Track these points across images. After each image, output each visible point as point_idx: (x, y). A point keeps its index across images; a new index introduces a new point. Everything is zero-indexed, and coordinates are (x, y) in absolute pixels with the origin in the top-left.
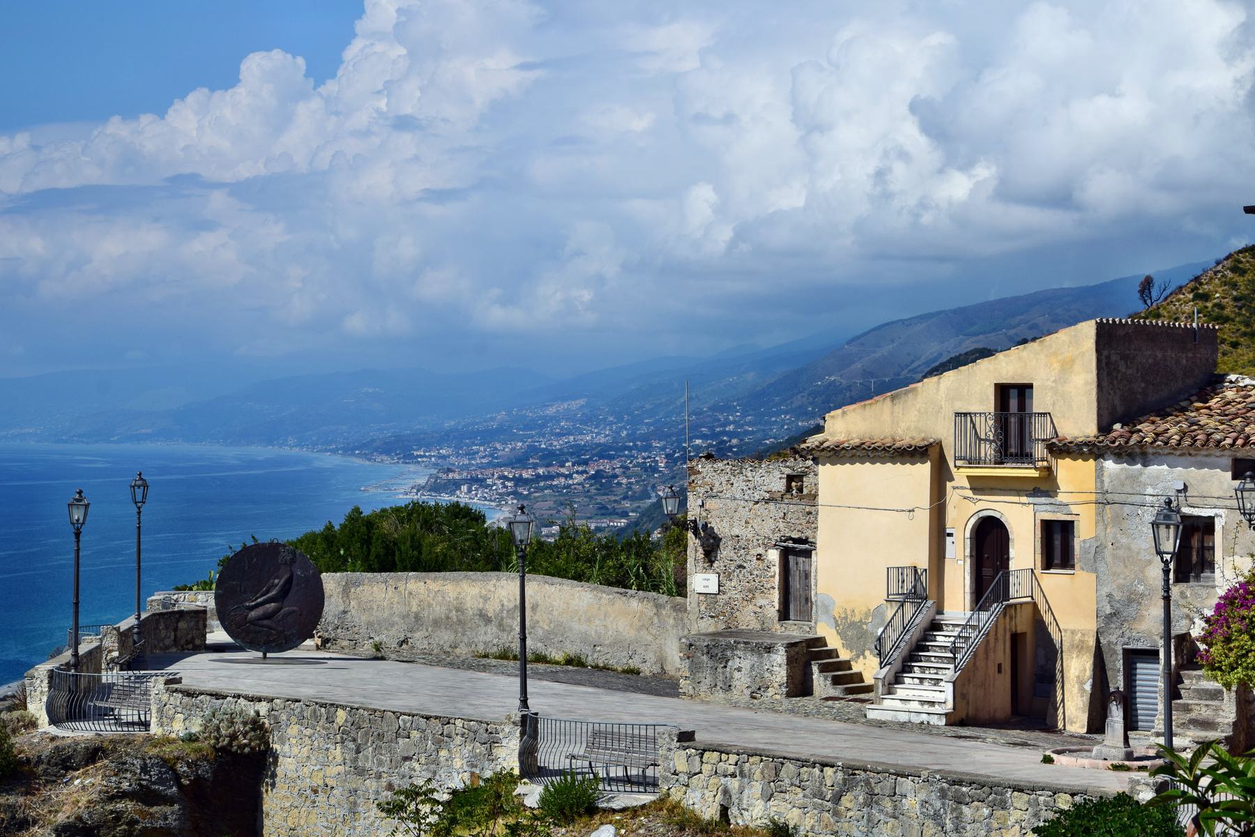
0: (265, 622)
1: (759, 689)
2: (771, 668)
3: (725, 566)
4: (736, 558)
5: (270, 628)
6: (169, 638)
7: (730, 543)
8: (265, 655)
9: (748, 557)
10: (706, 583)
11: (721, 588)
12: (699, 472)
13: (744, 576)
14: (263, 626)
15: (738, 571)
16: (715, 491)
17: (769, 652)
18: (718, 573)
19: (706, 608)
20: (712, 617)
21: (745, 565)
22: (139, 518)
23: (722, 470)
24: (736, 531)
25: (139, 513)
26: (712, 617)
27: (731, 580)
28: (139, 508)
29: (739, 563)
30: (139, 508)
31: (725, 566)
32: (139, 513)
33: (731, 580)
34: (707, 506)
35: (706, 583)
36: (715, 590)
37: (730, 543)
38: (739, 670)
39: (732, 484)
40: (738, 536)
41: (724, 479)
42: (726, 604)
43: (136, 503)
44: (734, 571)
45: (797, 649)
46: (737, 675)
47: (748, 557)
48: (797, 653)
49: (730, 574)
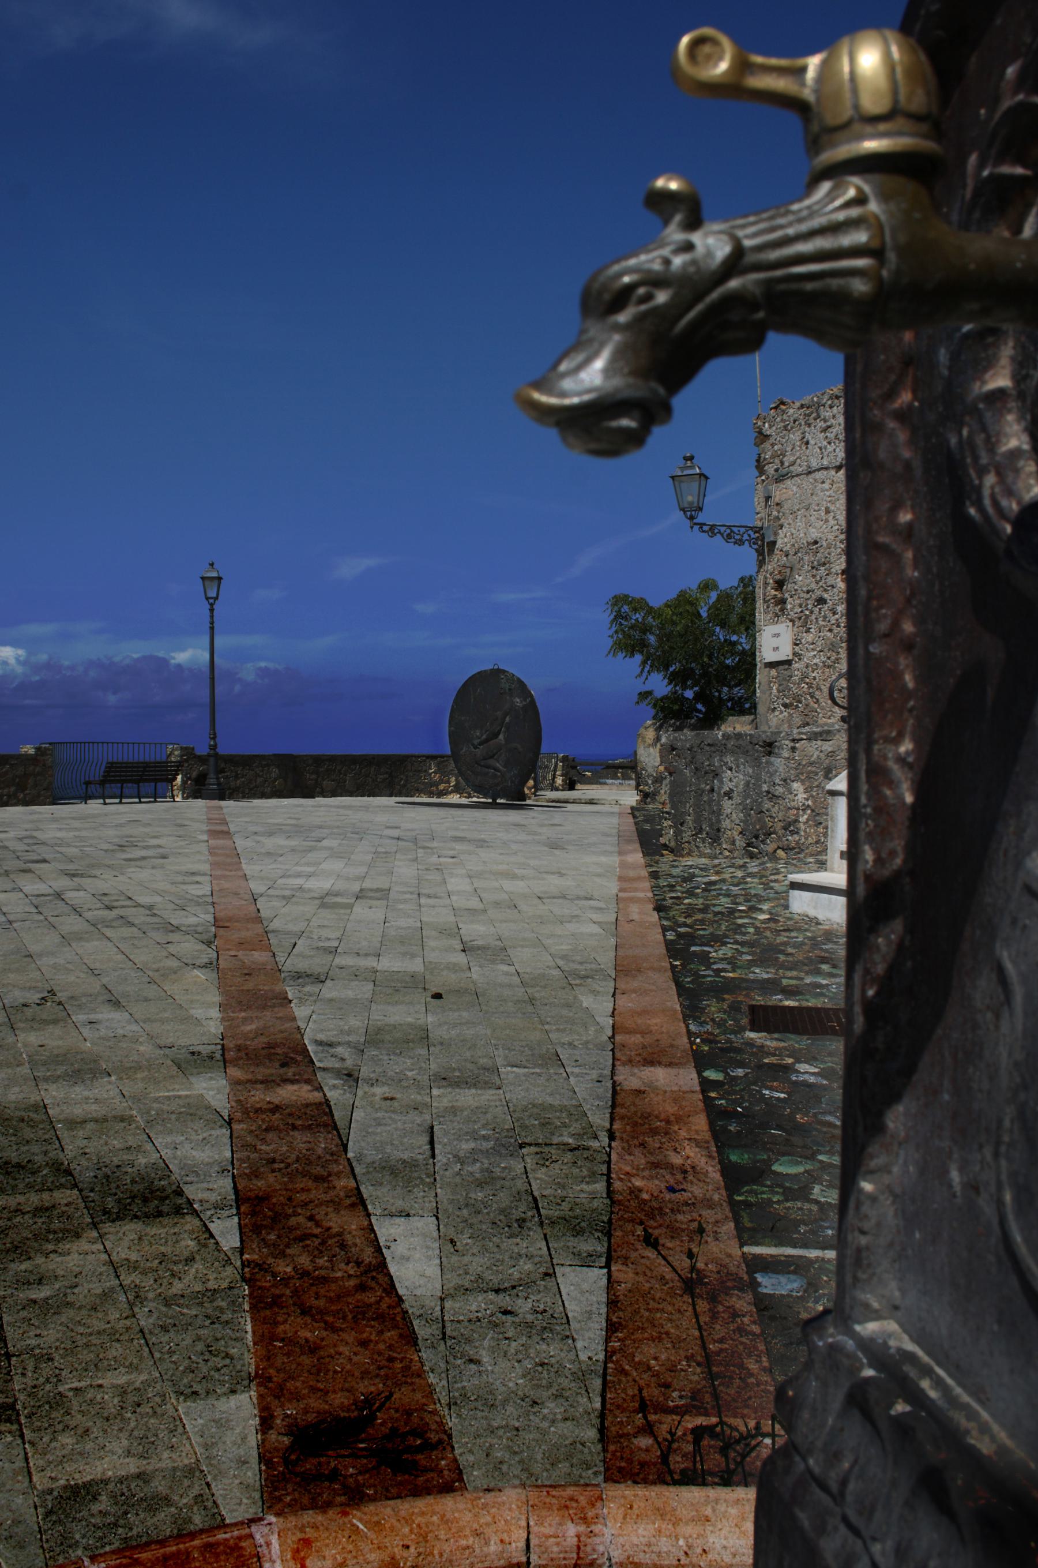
0: (491, 762)
1: (757, 837)
2: (772, 789)
3: (800, 606)
4: (813, 586)
5: (496, 769)
6: (448, 782)
7: (806, 558)
8: (494, 800)
9: (830, 580)
10: (775, 642)
11: (797, 648)
12: (768, 437)
13: (825, 617)
14: (488, 767)
15: (816, 610)
16: (786, 464)
17: (770, 753)
18: (791, 620)
19: (779, 691)
20: (785, 706)
21: (826, 596)
22: (212, 617)
23: (795, 421)
24: (814, 535)
25: (212, 610)
26: (785, 706)
27: (808, 631)
28: (212, 605)
29: (819, 593)
30: (212, 605)
31: (800, 606)
32: (212, 610)
33: (808, 631)
34: (777, 497)
35: (775, 642)
36: (785, 652)
37: (806, 558)
38: (729, 795)
39: (807, 443)
40: (816, 542)
41: (795, 437)
42: (804, 676)
43: (207, 599)
44: (812, 612)
45: (827, 746)
46: (727, 805)
47: (830, 580)
48: (831, 754)
49: (807, 617)
